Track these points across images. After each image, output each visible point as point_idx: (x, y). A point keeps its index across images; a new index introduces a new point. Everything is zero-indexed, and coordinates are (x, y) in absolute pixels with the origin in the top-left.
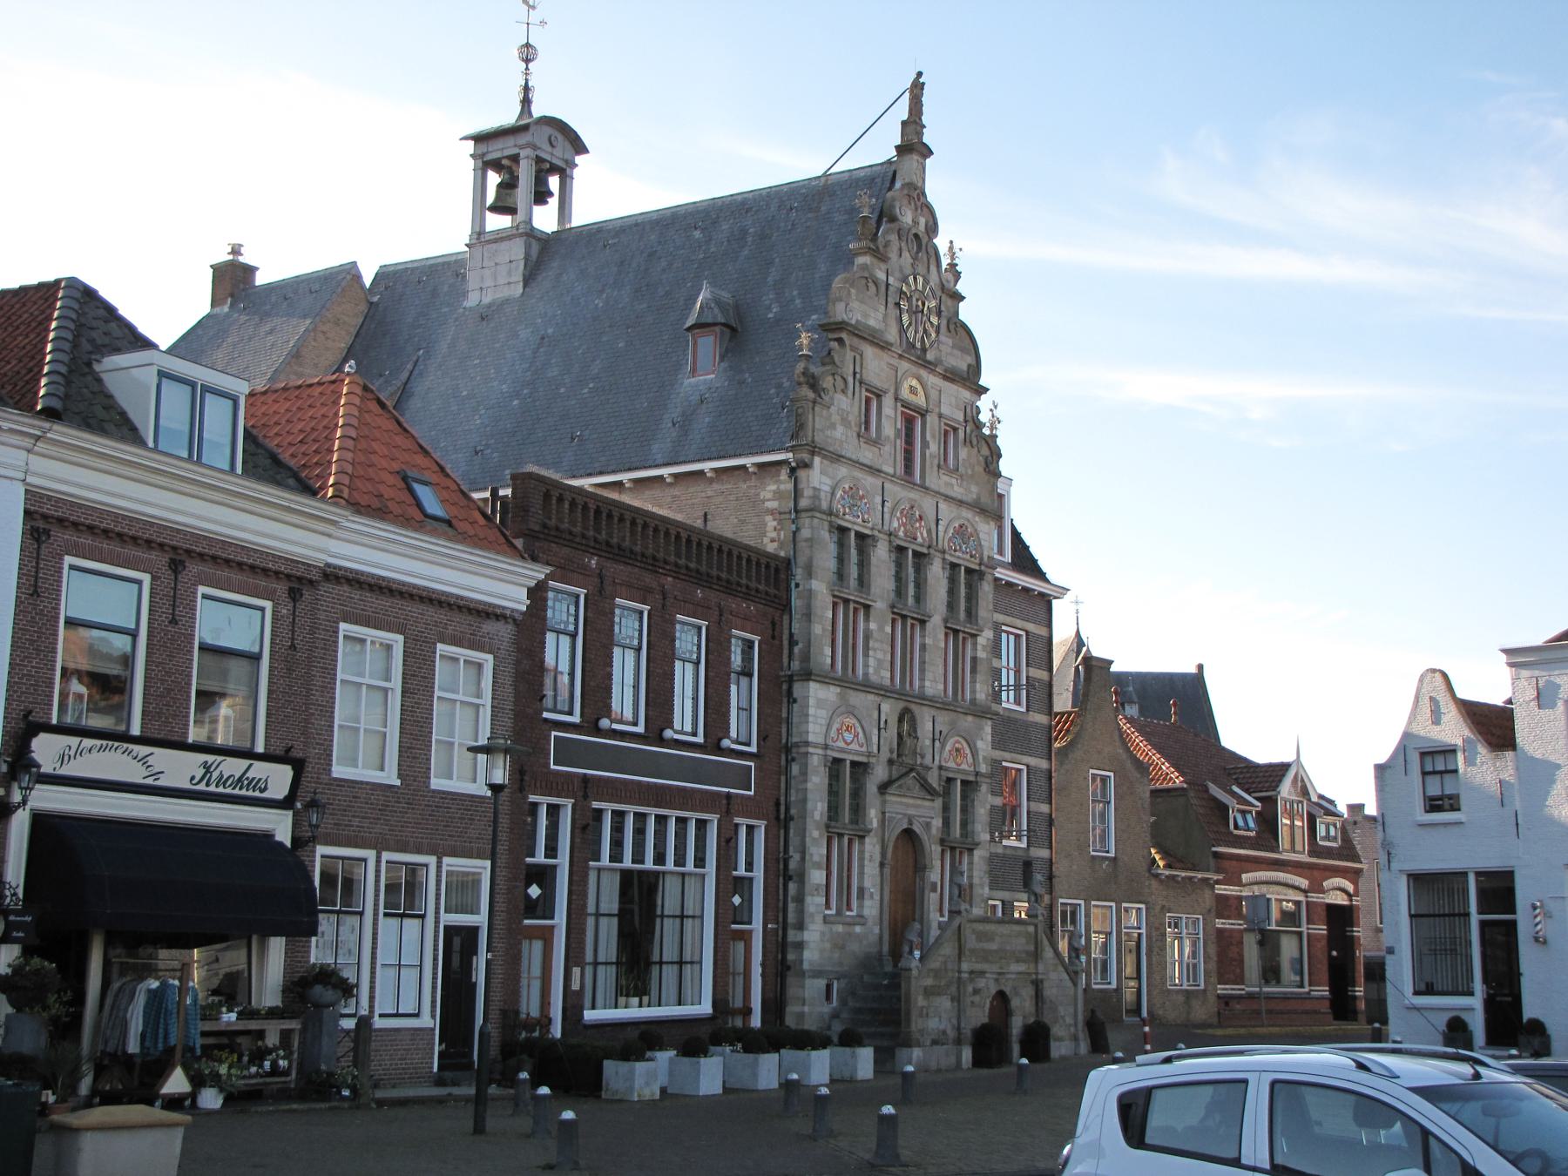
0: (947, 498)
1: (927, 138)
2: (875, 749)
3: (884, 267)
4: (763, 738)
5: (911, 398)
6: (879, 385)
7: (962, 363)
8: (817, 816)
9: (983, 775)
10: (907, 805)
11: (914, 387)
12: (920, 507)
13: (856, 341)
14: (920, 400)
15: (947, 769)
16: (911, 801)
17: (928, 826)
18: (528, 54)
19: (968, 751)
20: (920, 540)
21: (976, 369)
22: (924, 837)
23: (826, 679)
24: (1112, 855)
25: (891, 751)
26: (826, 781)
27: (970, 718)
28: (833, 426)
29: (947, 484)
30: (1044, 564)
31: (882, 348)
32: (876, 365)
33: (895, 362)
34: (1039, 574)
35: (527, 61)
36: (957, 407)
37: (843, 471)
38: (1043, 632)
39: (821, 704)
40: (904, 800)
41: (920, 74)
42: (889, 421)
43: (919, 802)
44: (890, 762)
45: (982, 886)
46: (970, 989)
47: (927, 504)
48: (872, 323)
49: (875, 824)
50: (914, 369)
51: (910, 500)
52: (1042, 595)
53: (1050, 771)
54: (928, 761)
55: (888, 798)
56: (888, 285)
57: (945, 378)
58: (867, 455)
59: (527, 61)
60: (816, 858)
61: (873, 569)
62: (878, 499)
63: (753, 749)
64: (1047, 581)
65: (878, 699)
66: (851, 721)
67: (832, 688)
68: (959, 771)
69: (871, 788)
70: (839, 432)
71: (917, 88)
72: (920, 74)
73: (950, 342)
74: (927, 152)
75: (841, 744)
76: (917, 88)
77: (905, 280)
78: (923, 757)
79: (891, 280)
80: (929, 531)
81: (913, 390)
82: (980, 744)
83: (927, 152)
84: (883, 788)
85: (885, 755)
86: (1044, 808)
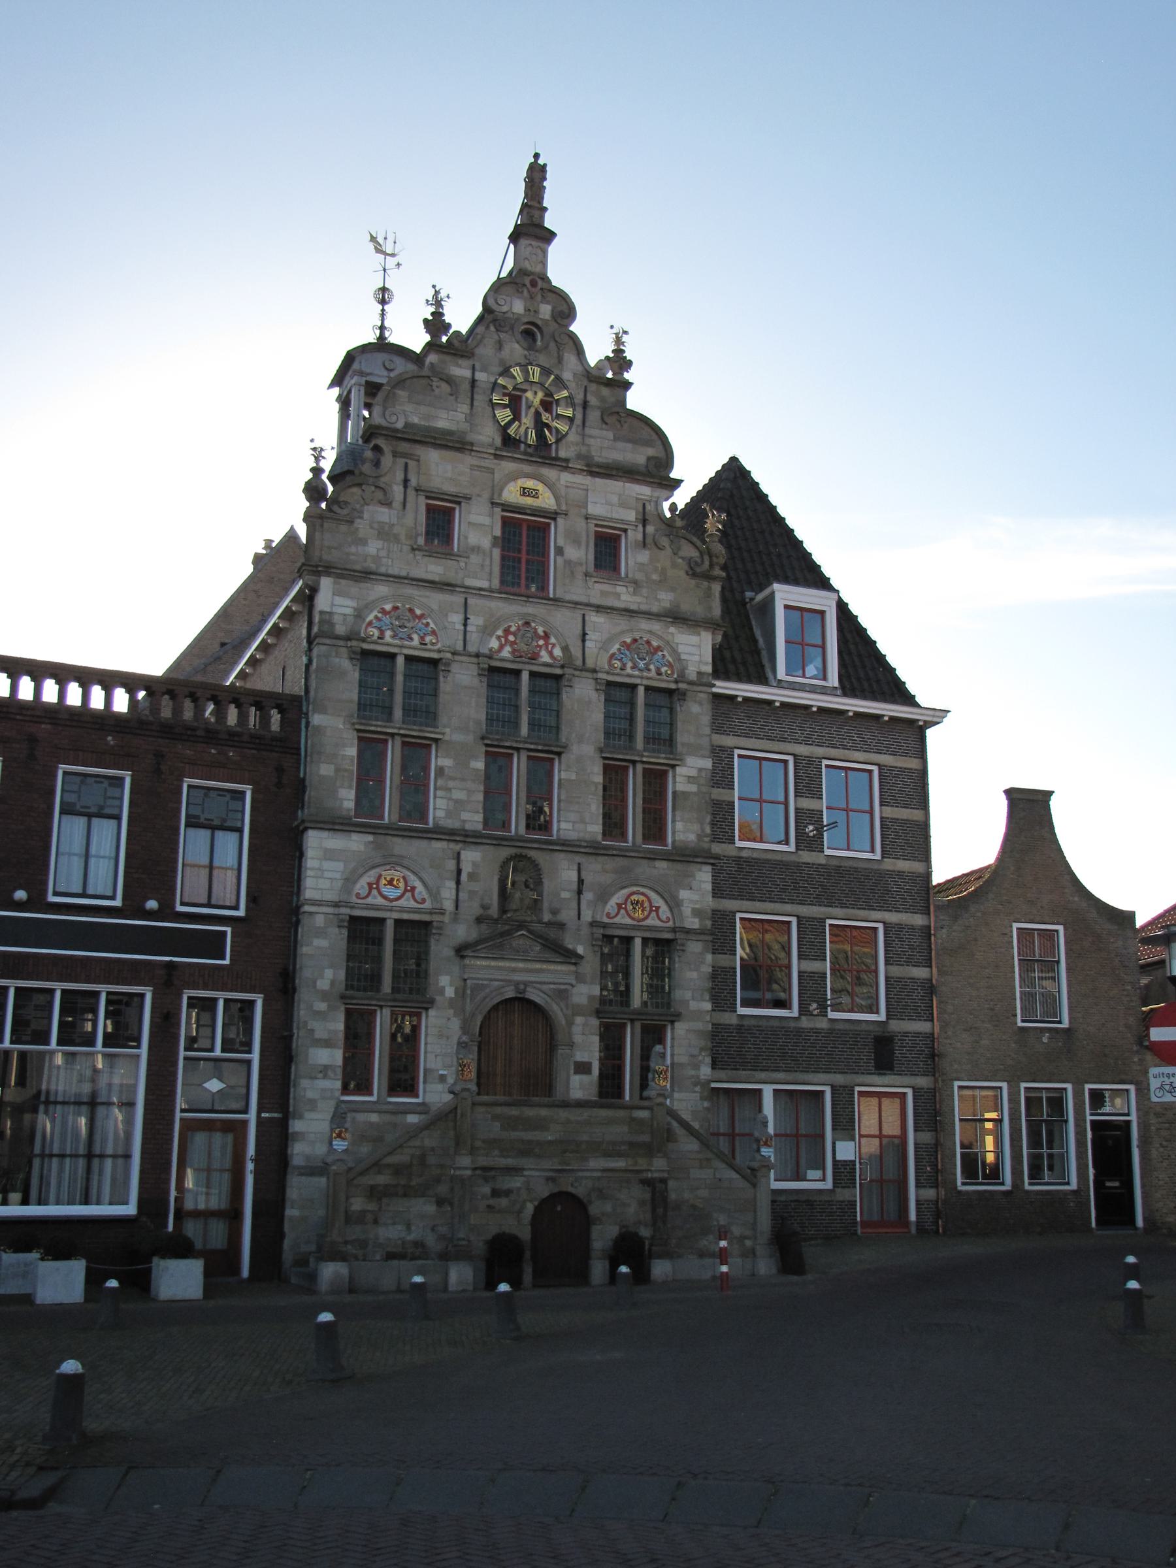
0: (599, 609)
1: (549, 222)
2: (449, 905)
3: (470, 362)
4: (252, 899)
5: (529, 501)
6: (450, 489)
7: (638, 457)
8: (323, 984)
9: (688, 931)
10: (514, 970)
11: (610, 501)
12: (544, 622)
13: (404, 447)
14: (546, 500)
15: (605, 926)
16: (521, 965)
17: (562, 995)
18: (383, 296)
19: (658, 901)
20: (545, 657)
21: (666, 458)
22: (557, 1010)
23: (338, 824)
24: (1065, 1024)
25: (485, 907)
26: (344, 944)
27: (662, 865)
28: (363, 542)
29: (603, 594)
30: (912, 688)
31: (460, 450)
32: (442, 470)
33: (489, 463)
34: (898, 692)
35: (383, 302)
36: (623, 505)
37: (382, 590)
38: (913, 764)
39: (329, 855)
40: (501, 964)
41: (537, 156)
42: (477, 528)
43: (538, 966)
44: (479, 920)
45: (696, 1067)
46: (487, 1190)
47: (565, 622)
48: (442, 424)
49: (450, 992)
50: (527, 468)
51: (521, 616)
52: (912, 722)
53: (929, 927)
54: (567, 915)
55: (467, 961)
56: (473, 382)
57: (592, 474)
58: (434, 569)
59: (383, 302)
60: (320, 1034)
61: (442, 698)
62: (456, 619)
63: (241, 913)
64: (917, 705)
65: (458, 847)
66: (396, 874)
67: (355, 836)
68: (633, 927)
69: (440, 950)
70: (374, 547)
71: (536, 176)
72: (537, 156)
73: (610, 435)
74: (550, 236)
75: (380, 901)
76: (536, 176)
77: (506, 372)
78: (555, 912)
79: (479, 376)
80: (565, 649)
81: (525, 492)
82: (684, 894)
83: (550, 236)
84: (461, 951)
85: (471, 909)
86: (920, 973)
